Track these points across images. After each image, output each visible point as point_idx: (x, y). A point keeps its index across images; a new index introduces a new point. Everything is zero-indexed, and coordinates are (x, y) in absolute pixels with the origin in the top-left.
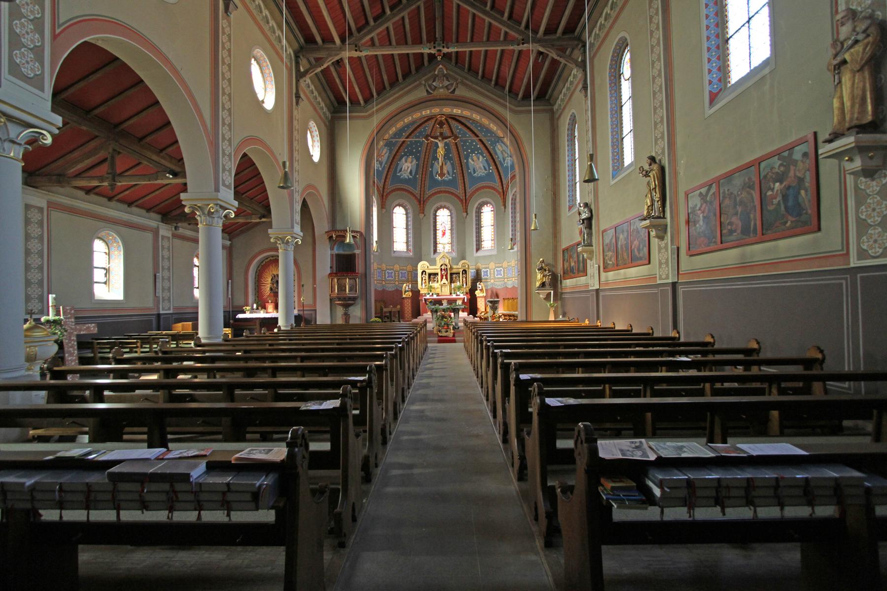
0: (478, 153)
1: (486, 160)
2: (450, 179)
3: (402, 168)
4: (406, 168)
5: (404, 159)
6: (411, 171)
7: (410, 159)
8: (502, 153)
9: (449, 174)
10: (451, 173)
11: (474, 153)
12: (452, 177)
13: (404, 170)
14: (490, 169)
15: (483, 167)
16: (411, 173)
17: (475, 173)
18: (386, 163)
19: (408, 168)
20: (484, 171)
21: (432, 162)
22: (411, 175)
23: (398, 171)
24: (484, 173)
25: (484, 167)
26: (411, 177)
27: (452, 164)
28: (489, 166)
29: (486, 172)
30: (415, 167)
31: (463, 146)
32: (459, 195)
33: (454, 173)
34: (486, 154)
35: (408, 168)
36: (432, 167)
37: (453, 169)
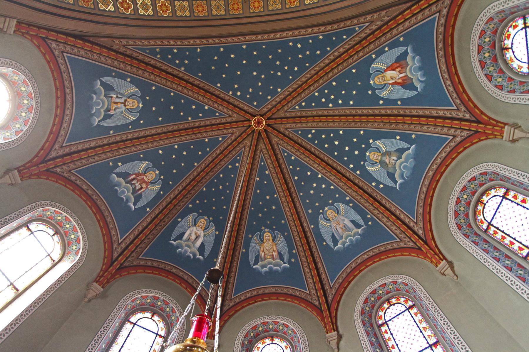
0: (335, 200)
1: (355, 208)
2: (285, 269)
3: (183, 234)
4: (193, 237)
5: (191, 217)
6: (202, 244)
7: (203, 222)
8: (383, 164)
9: (281, 258)
10: (286, 256)
11: (328, 205)
12: (290, 263)
13: (188, 239)
14: (366, 221)
15: (350, 225)
16: (202, 249)
17: (335, 242)
18: (150, 204)
19: (197, 237)
20: (356, 230)
21: (247, 234)
22: (202, 254)
23: (174, 236)
24: (357, 233)
25: (353, 222)
26: (201, 257)
27: (288, 239)
28: (363, 214)
29: (360, 230)
30: (212, 239)
31: (304, 199)
32: (309, 298)
33: (291, 255)
34: (350, 193)
35: (197, 237)
36: (247, 245)
37: (290, 247)
